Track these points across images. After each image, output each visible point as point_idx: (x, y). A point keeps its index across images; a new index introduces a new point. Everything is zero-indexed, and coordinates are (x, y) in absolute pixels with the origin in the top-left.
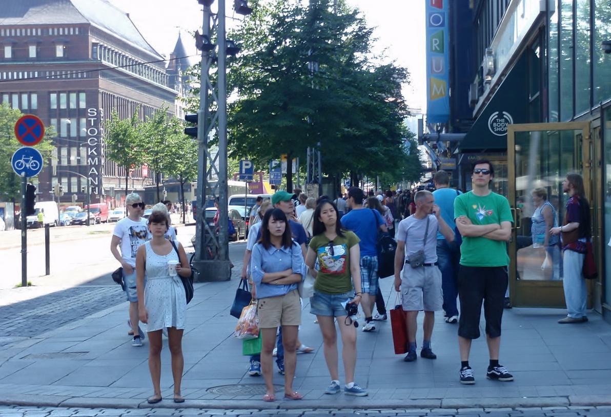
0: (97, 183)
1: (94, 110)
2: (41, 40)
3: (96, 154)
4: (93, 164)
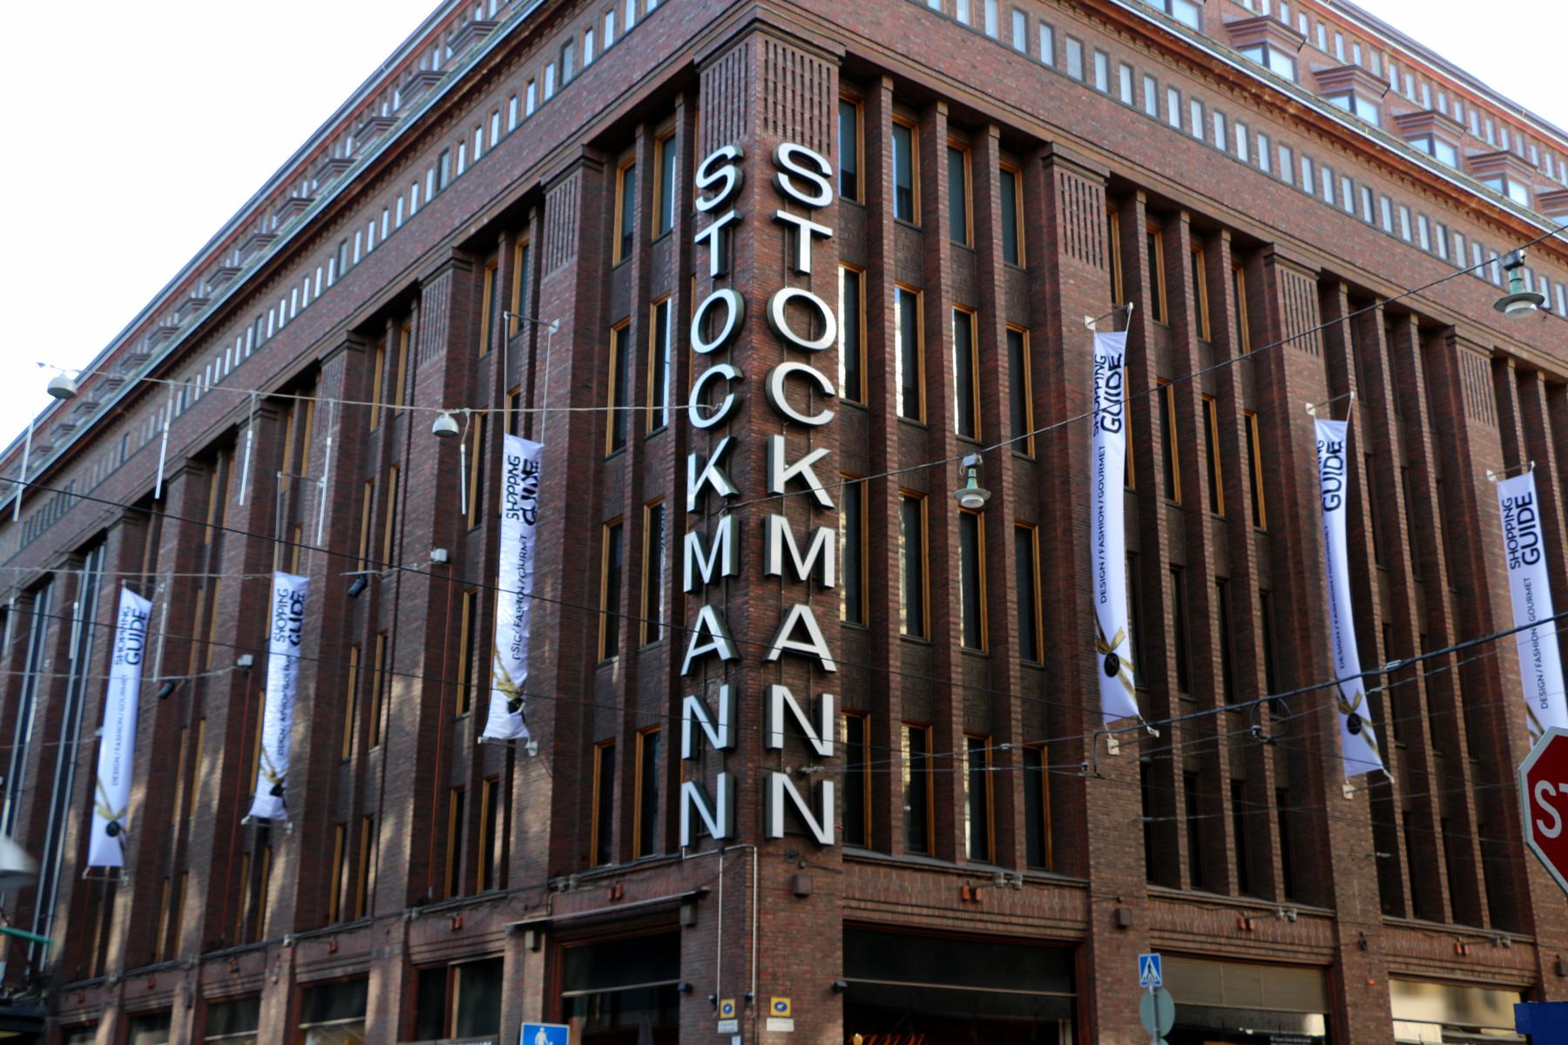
1: (722, 161)
3: (722, 487)
4: (707, 575)
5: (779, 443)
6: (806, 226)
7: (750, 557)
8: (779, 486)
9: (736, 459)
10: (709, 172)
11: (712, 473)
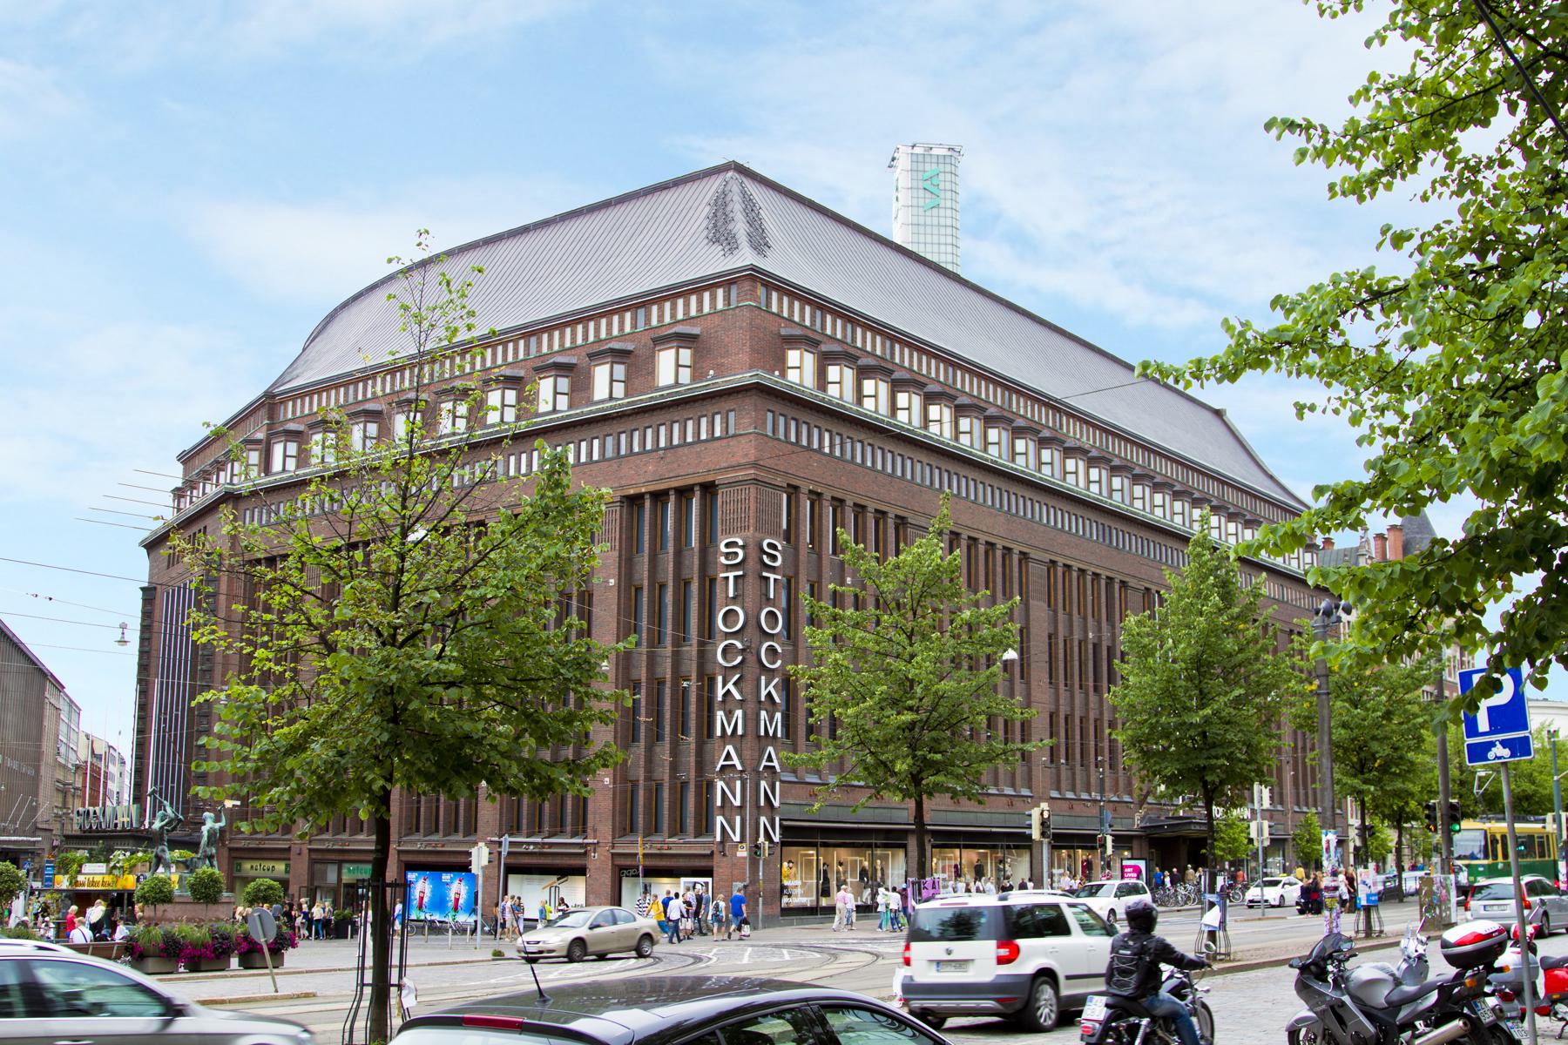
0: (737, 803)
1: (733, 544)
2: (630, 347)
3: (738, 697)
4: (729, 731)
5: (763, 678)
6: (772, 577)
7: (751, 725)
8: (763, 699)
9: (742, 684)
10: (727, 545)
11: (730, 686)
